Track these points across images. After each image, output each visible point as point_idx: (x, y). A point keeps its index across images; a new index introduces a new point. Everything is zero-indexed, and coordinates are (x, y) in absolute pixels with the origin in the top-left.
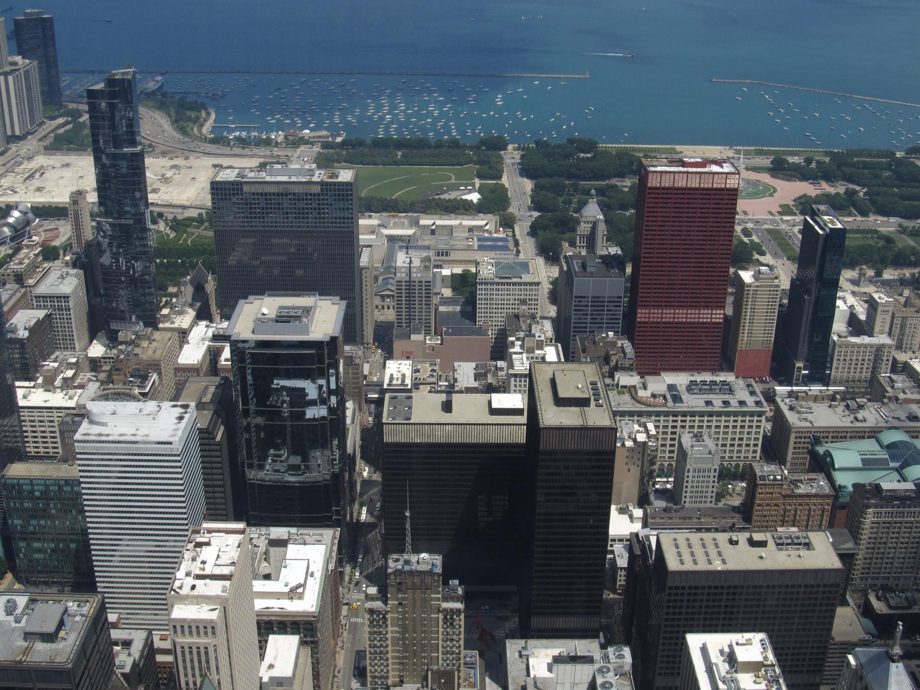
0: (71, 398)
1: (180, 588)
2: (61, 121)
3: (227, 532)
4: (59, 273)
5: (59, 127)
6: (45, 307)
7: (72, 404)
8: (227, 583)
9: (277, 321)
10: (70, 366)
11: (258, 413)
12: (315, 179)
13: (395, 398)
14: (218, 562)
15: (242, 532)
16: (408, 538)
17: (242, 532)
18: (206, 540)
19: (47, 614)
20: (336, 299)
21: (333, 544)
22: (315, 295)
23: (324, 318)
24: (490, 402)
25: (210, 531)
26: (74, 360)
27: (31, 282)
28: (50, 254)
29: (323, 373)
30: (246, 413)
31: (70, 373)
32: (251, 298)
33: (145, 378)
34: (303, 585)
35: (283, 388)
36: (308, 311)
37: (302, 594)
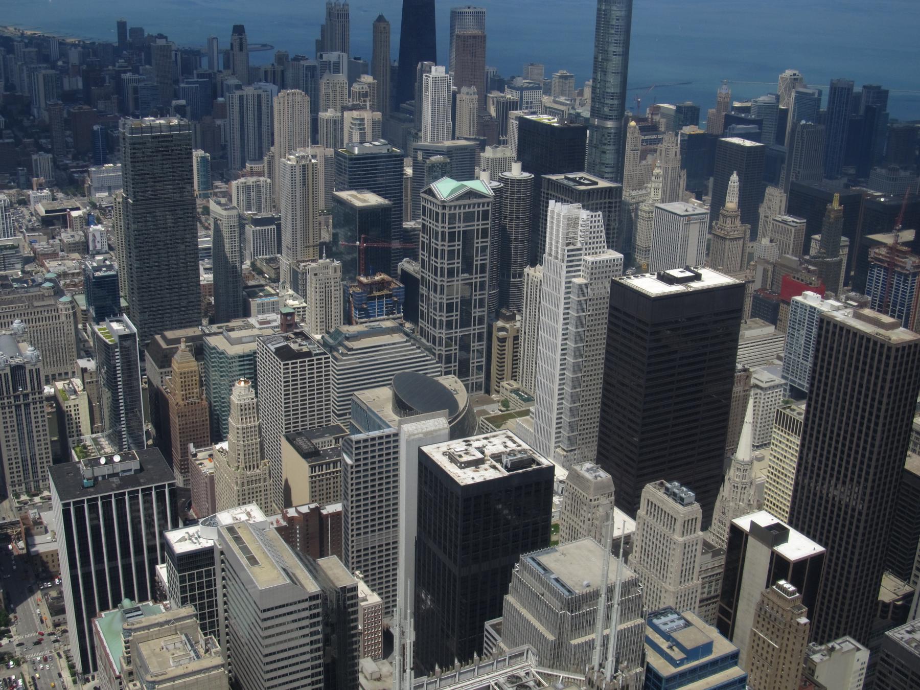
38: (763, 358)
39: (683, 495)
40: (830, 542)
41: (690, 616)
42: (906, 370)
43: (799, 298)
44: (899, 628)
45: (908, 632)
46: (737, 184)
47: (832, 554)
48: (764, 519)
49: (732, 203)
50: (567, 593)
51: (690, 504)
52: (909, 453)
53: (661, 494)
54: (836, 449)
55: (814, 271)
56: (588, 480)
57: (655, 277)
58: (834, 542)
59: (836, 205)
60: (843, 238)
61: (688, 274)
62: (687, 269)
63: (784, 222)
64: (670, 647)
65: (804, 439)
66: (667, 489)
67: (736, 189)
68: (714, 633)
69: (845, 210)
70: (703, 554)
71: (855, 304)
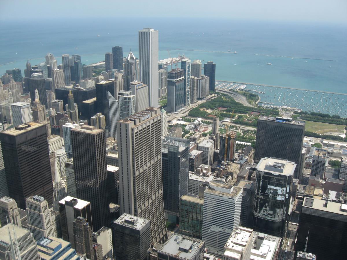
0: (204, 179)
1: (229, 245)
2: (213, 95)
3: (247, 231)
4: (207, 141)
5: (213, 97)
6: (201, 150)
7: (204, 181)
8: (244, 248)
9: (273, 167)
10: (206, 169)
11: (261, 195)
12: (291, 123)
13: (307, 198)
14: (242, 240)
15: (251, 232)
16: (306, 247)
17: (251, 232)
18: (239, 232)
19: (187, 244)
20: (293, 163)
21: (278, 243)
22: (286, 160)
23: (289, 168)
24: (341, 207)
25: (241, 230)
26: (207, 168)
27: (198, 142)
28: (205, 135)
29: (285, 186)
30: (258, 194)
31: (205, 172)
32: (266, 158)
33: (227, 177)
34: (267, 254)
35: (271, 189)
36: (283, 165)
37: (266, 257)
38: (58, 147)
39: (40, 199)
40: (91, 200)
41: (51, 238)
42: (100, 141)
43: (64, 126)
44: (117, 220)
45: (121, 220)
46: (38, 93)
47: (92, 203)
48: (69, 198)
49: (37, 100)
50: (6, 245)
51: (43, 201)
52: (107, 165)
53: (32, 200)
54: (85, 171)
55: (68, 116)
56: (6, 203)
57: (15, 129)
58: (92, 199)
59: (71, 94)
60: (75, 104)
61: (26, 125)
62: (25, 124)
63: (56, 102)
64: (47, 250)
65: (75, 170)
66: (34, 199)
67: (38, 94)
68: (61, 240)
69: (74, 95)
70: (52, 216)
71: (83, 124)
